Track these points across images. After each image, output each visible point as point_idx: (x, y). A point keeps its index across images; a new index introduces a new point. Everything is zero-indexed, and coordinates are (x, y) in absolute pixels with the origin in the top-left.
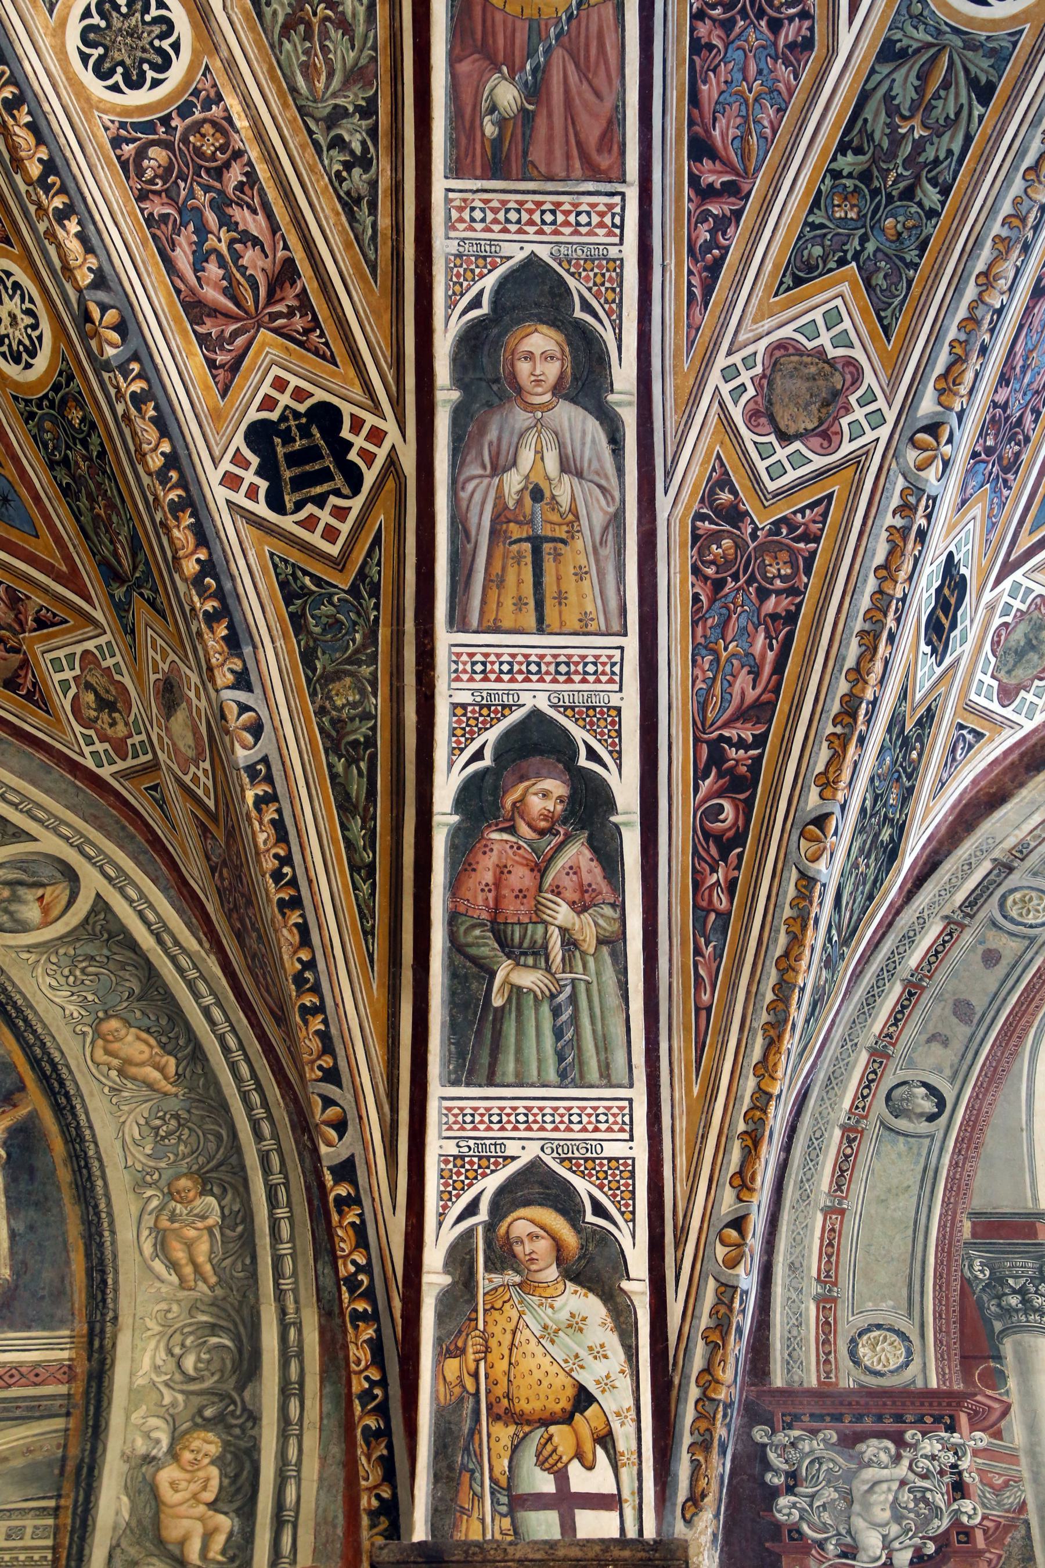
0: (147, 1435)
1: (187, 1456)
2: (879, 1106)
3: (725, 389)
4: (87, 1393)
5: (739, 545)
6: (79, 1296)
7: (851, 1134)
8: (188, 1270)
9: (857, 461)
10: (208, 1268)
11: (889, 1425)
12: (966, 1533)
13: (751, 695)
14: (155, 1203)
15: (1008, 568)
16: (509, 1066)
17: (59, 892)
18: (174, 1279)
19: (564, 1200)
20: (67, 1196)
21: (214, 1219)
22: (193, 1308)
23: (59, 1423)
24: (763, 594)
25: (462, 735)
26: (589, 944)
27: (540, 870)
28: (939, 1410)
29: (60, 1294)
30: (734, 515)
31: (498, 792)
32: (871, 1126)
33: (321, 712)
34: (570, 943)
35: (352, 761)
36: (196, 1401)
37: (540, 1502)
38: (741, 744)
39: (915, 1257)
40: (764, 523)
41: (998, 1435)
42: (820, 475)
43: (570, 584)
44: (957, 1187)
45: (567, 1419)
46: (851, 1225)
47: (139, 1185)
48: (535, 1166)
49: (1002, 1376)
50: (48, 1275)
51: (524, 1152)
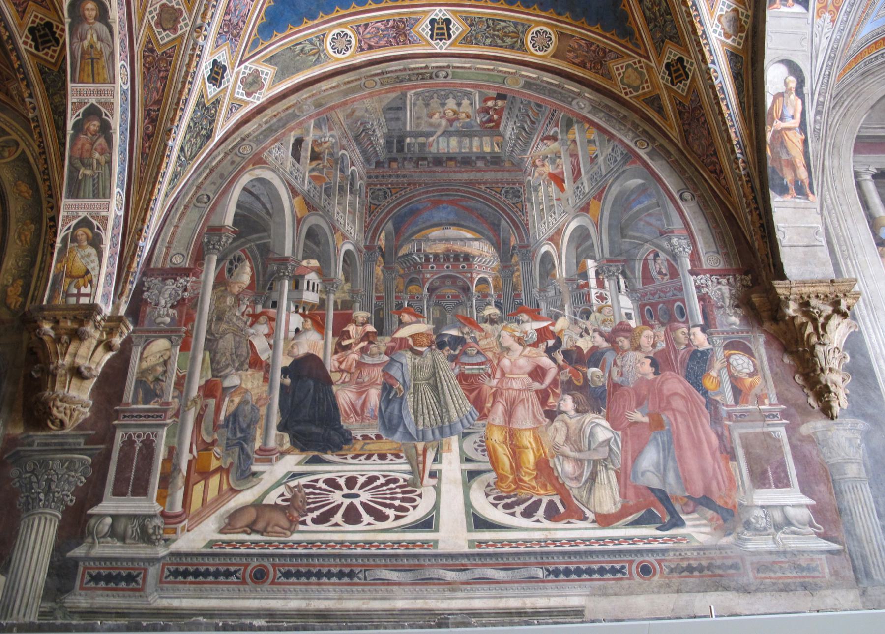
2: (195, 200)
3: (150, 17)
5: (154, 59)
7: (186, 207)
9: (182, 36)
11: (174, 276)
12: (183, 299)
13: (157, 98)
15: (241, 63)
16: (81, 194)
19: (90, 225)
24: (160, 71)
25: (74, 110)
26: (103, 163)
27: (92, 144)
28: (185, 272)
30: (152, 50)
31: (82, 125)
32: (191, 205)
33: (51, 104)
34: (98, 163)
35: (59, 116)
37: (73, 295)
38: (154, 111)
39: (192, 237)
40: (160, 53)
41: (198, 277)
42: (173, 40)
43: (101, 71)
44: (207, 220)
45: (83, 277)
46: (180, 229)
48: (85, 218)
49: (203, 264)
51: (82, 214)
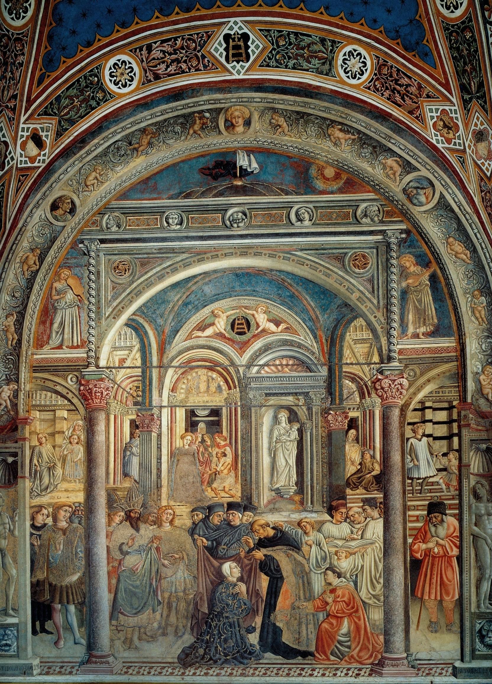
0: (476, 366)
1: (486, 372)
4: (461, 355)
6: (455, 328)
8: (480, 320)
10: (485, 319)
14: (470, 299)
17: (430, 191)
18: (477, 322)
20: (447, 297)
21: (485, 304)
22: (483, 332)
23: (455, 363)
29: (450, 327)
36: (486, 357)
47: (465, 293)
50: (446, 321)
